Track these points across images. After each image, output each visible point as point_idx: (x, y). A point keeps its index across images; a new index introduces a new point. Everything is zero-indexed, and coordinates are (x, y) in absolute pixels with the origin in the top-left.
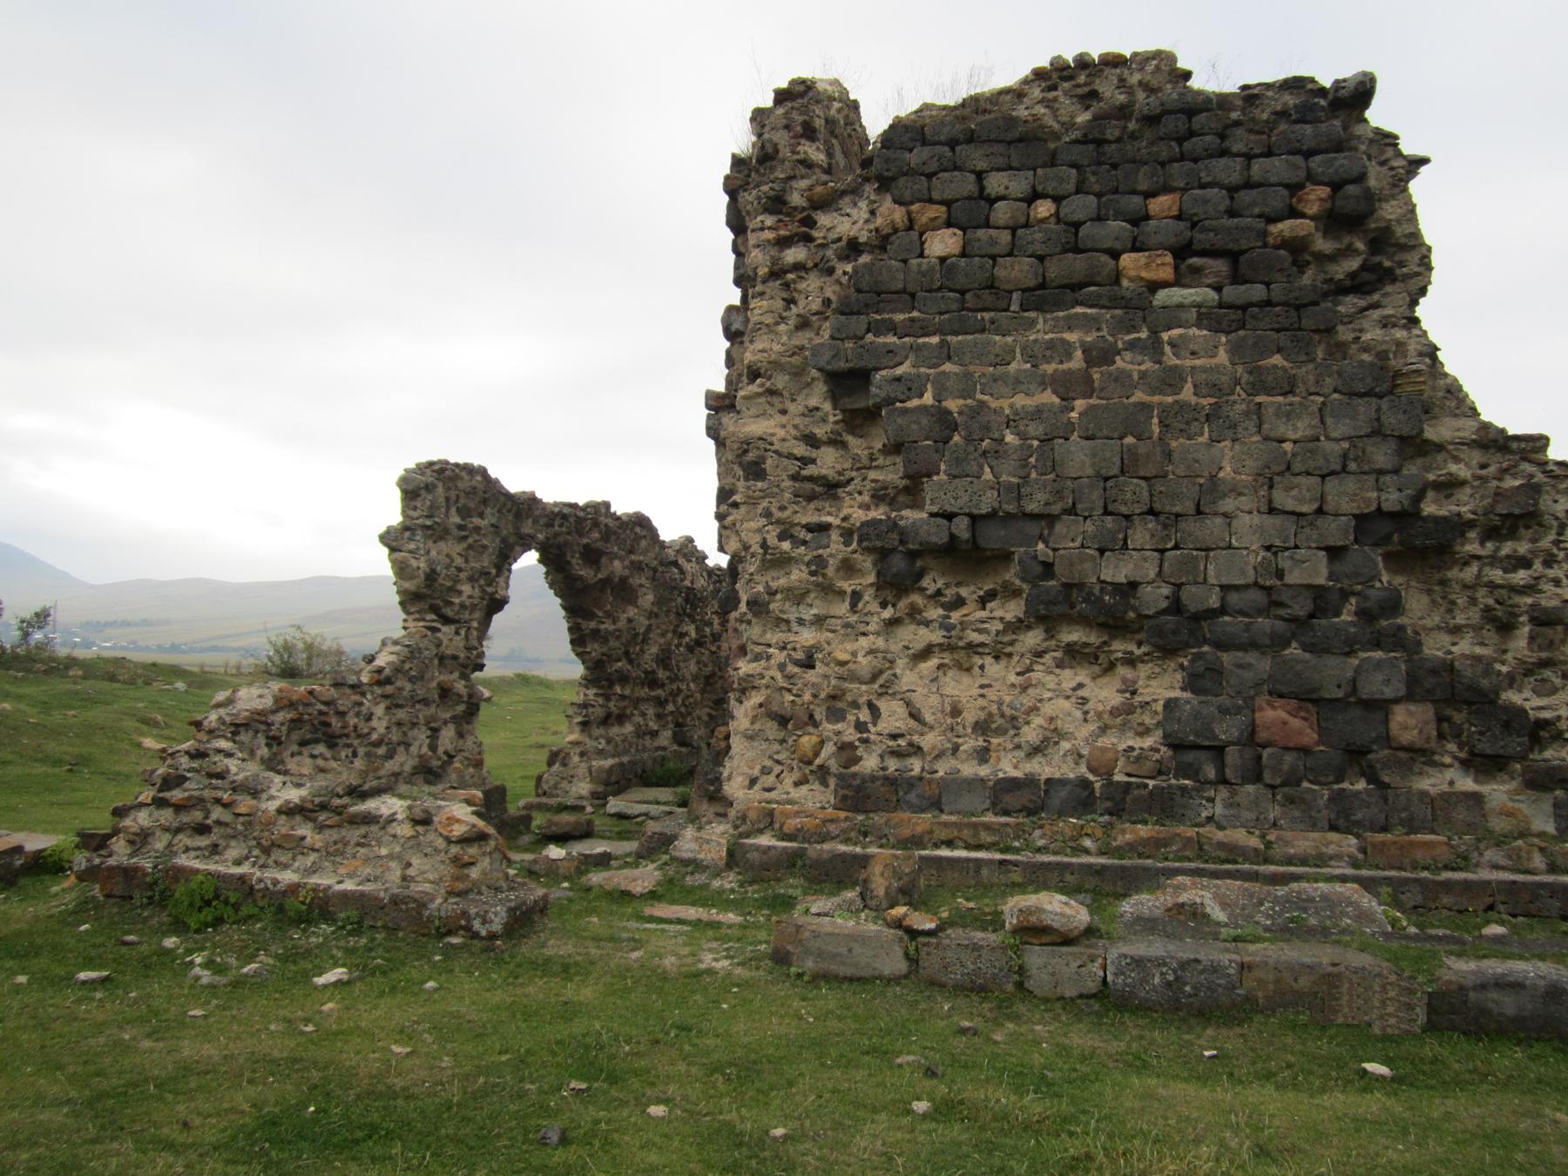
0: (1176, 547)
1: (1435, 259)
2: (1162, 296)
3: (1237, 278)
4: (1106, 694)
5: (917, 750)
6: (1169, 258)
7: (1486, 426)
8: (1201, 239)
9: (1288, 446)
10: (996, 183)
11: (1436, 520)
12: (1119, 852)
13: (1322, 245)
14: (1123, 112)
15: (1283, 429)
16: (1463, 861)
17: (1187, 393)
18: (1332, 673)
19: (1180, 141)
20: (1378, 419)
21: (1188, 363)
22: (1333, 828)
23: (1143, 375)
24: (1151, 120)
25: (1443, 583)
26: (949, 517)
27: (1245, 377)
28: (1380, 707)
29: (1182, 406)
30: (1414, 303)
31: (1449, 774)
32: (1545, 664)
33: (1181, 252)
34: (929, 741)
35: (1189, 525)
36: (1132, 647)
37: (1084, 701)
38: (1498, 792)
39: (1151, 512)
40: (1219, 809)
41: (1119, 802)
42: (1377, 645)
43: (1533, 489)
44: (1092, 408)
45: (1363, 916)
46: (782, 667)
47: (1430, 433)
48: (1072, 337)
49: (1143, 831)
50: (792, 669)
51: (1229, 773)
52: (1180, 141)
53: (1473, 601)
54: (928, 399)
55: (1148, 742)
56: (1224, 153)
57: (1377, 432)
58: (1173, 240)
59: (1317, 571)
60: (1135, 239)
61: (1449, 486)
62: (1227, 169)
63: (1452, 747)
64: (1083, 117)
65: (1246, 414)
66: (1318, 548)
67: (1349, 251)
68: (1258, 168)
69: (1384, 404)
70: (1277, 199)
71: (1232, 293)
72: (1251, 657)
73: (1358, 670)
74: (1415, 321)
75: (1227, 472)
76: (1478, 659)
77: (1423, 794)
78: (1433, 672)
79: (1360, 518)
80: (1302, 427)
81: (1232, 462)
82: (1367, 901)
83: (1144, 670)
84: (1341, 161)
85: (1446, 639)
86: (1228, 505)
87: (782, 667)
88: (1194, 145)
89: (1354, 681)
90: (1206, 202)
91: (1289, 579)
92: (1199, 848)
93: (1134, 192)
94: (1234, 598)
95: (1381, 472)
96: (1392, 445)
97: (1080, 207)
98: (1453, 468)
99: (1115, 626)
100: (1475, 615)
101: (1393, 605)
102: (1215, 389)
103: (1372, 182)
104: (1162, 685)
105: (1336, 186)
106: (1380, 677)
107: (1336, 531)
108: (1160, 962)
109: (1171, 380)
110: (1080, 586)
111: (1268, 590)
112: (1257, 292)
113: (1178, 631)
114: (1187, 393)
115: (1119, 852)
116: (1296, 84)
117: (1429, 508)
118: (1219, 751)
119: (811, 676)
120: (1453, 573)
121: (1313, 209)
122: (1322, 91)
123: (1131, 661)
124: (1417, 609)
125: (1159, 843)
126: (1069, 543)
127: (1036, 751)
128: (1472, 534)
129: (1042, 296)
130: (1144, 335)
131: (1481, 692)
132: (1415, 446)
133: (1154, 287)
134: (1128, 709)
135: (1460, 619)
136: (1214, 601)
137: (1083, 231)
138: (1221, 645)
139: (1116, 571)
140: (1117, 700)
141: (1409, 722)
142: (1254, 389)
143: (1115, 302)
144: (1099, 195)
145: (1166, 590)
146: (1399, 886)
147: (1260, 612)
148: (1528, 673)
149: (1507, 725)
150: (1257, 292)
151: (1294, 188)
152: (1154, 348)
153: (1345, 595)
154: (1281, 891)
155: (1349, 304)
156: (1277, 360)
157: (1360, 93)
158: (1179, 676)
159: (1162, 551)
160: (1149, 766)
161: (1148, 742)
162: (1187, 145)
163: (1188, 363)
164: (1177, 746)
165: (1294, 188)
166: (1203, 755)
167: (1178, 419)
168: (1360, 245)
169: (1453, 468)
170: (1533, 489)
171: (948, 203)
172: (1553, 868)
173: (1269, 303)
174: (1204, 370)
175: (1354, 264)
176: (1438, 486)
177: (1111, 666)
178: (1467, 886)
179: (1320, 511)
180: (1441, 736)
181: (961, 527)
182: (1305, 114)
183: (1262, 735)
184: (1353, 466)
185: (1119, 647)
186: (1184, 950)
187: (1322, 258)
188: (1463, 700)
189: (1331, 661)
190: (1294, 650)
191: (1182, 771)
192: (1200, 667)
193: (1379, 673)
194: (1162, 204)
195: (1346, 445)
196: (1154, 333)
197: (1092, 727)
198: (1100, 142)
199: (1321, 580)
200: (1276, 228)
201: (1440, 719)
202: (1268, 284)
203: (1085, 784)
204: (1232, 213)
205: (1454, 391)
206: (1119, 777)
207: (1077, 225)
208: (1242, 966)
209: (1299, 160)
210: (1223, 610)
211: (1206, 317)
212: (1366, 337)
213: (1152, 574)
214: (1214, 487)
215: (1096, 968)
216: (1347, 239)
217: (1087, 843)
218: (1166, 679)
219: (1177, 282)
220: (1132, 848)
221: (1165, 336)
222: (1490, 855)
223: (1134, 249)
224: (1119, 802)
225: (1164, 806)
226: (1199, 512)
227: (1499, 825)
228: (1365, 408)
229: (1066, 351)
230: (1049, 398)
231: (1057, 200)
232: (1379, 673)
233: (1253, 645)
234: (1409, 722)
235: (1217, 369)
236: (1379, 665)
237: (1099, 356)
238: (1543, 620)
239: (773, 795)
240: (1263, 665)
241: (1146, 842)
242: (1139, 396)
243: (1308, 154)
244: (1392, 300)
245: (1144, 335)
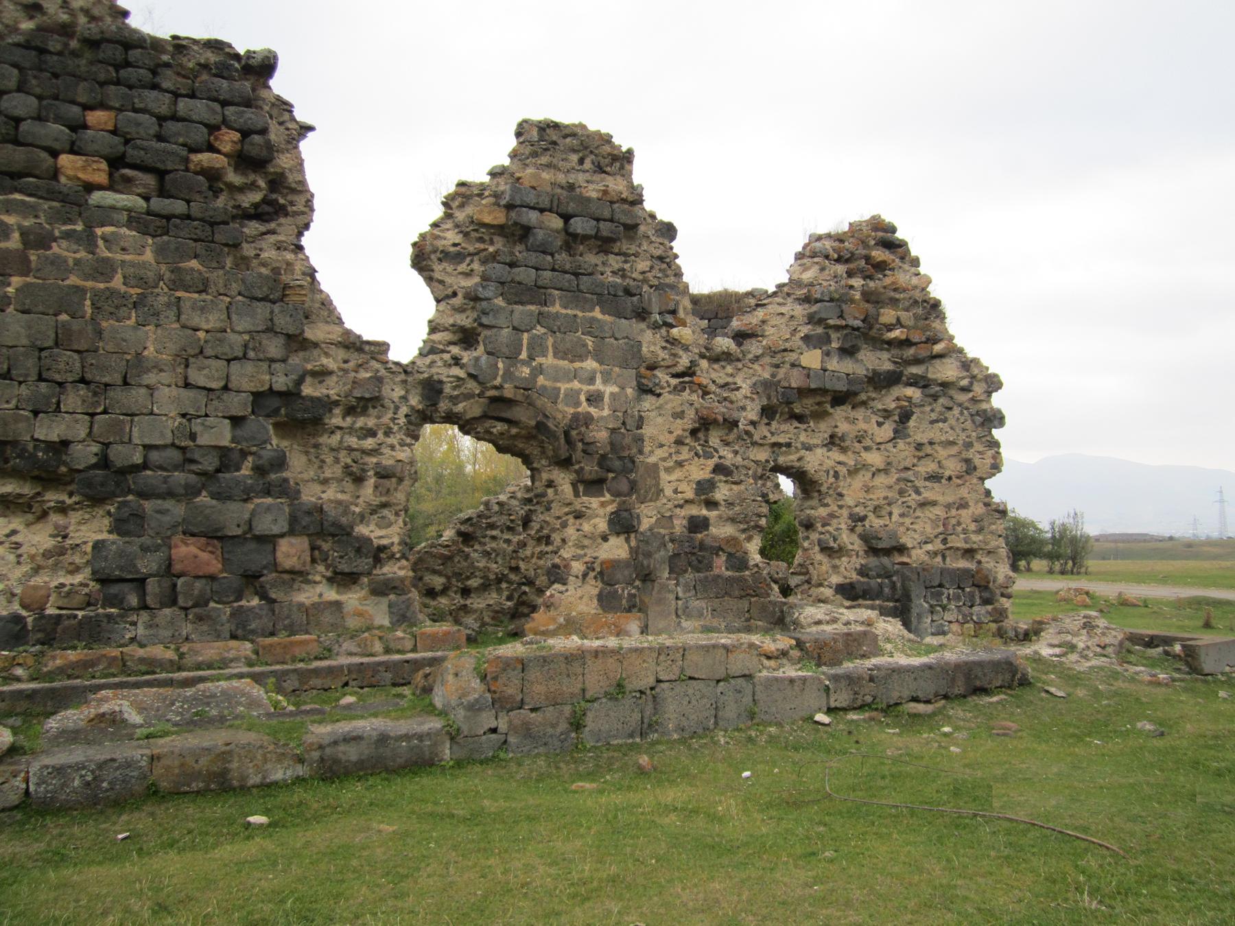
0: (105, 412)
1: (316, 203)
2: (97, 197)
3: (163, 193)
4: (39, 538)
6: (104, 165)
7: (348, 333)
8: (132, 154)
9: (201, 334)
11: (312, 399)
12: (50, 676)
13: (233, 177)
14: (66, 30)
15: (197, 320)
16: (328, 653)
17: (117, 282)
18: (233, 515)
19: (117, 67)
20: (271, 320)
21: (119, 257)
22: (234, 637)
23: (77, 262)
24: (93, 44)
25: (316, 446)
27: (167, 275)
28: (269, 541)
29: (112, 293)
30: (300, 234)
31: (319, 589)
32: (384, 505)
33: (116, 162)
35: (117, 394)
36: (64, 497)
37: (18, 545)
38: (353, 599)
39: (83, 380)
40: (141, 630)
41: (51, 633)
42: (268, 493)
43: (379, 380)
44: (27, 285)
45: (253, 703)
47: (309, 334)
48: (11, 220)
49: (72, 655)
51: (150, 600)
52: (117, 67)
53: (337, 460)
55: (78, 579)
56: (155, 87)
57: (270, 330)
58: (107, 151)
59: (220, 434)
60: (73, 143)
61: (322, 374)
62: (159, 102)
63: (321, 568)
64: (27, 25)
65: (168, 305)
66: (224, 417)
67: (253, 186)
68: (183, 105)
69: (277, 308)
70: (199, 135)
71: (157, 204)
72: (168, 504)
73: (253, 513)
74: (300, 248)
75: (150, 352)
76: (339, 503)
77: (301, 605)
78: (309, 513)
79: (257, 395)
80: (213, 320)
81: (155, 343)
82: (257, 691)
83: (75, 517)
84: (249, 114)
85: (317, 488)
86: (151, 378)
89: (250, 522)
90: (138, 124)
91: (200, 441)
92: (123, 665)
93: (73, 102)
94: (154, 456)
95: (272, 360)
96: (280, 341)
98: (325, 361)
99: (47, 478)
100: (338, 471)
101: (280, 462)
102: (142, 281)
103: (272, 137)
104: (90, 529)
105: (245, 134)
106: (269, 517)
107: (238, 404)
108: (79, 767)
109: (103, 270)
110: (14, 443)
111: (183, 449)
112: (179, 207)
113: (106, 482)
114: (117, 282)
115: (50, 676)
116: (215, 45)
117: (308, 390)
118: (141, 582)
120: (324, 439)
121: (227, 148)
122: (237, 57)
123: (63, 509)
124: (298, 466)
125: (86, 665)
128: (337, 411)
130: (79, 227)
131: (340, 527)
132: (297, 342)
133: (90, 188)
134: (61, 551)
135: (328, 474)
136: (138, 458)
137: (24, 126)
138: (143, 495)
139: (48, 430)
140: (49, 543)
141: (291, 551)
142: (176, 285)
143: (51, 195)
144: (40, 98)
145: (95, 448)
146: (281, 676)
147: (176, 468)
148: (373, 512)
149: (358, 551)
150: (179, 207)
151: (213, 128)
152: (88, 240)
153: (244, 454)
154: (189, 692)
155: (253, 228)
156: (194, 264)
157: (263, 67)
158: (107, 521)
159: (92, 415)
160: (78, 600)
161: (78, 579)
162: (123, 73)
163: (119, 257)
164: (104, 581)
165: (213, 128)
166: (126, 587)
167: (109, 303)
168: (262, 183)
169: (325, 361)
170: (379, 380)
172: (388, 651)
173: (188, 217)
174: (133, 264)
175: (257, 197)
176: (314, 374)
177: (44, 515)
178: (331, 671)
179: (226, 388)
180: (313, 561)
182: (222, 71)
183: (177, 568)
184: (251, 354)
185: (52, 497)
186: (99, 754)
187: (231, 188)
188: (327, 532)
189: (233, 506)
190: (204, 499)
191: (109, 601)
192: (126, 512)
193: (269, 515)
194: (97, 118)
195: (247, 337)
196: (89, 227)
197: (25, 568)
198: (42, 51)
199: (225, 442)
201: (313, 548)
202: (188, 202)
203: (17, 619)
204: (160, 138)
205: (326, 304)
206: (51, 611)
207: (18, 120)
208: (152, 758)
209: (217, 106)
210: (145, 466)
211: (135, 220)
212: (264, 255)
213: (83, 434)
214: (138, 363)
215: (18, 783)
216: (252, 177)
217: (19, 672)
218: (95, 524)
219: (110, 187)
220: (61, 671)
221: (99, 231)
222: (348, 645)
223: (72, 151)
224: (51, 633)
225: (92, 632)
226: (125, 383)
227: (352, 623)
228: (262, 310)
232: (269, 515)
233: (170, 494)
234: (291, 551)
235: (143, 265)
236: (269, 509)
237: (37, 240)
238: (383, 474)
240: (178, 510)
241: (73, 665)
242: (73, 280)
243: (225, 104)
244: (285, 227)
245: (79, 227)
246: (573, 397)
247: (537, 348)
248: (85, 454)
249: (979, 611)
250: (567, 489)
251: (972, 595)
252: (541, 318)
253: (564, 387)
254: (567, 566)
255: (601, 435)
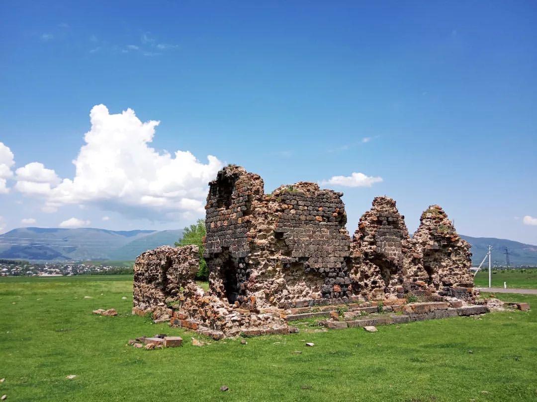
3: (329, 221)
5: (289, 298)
10: (300, 203)
26: (295, 257)
33: (323, 216)
34: (291, 296)
46: (267, 285)
50: (269, 285)
54: (292, 238)
56: (327, 202)
87: (267, 285)
88: (324, 200)
97: (311, 208)
119: (273, 286)
123: (316, 280)
126: (310, 262)
127: (305, 296)
129: (307, 222)
136: (329, 270)
167: (324, 242)
171: (293, 205)
181: (297, 259)
194: (320, 209)
200: (334, 214)
229: (309, 231)
230: (308, 238)
231: (308, 207)
239: (265, 309)
246: (391, 254)
247: (385, 245)
248: (322, 270)
249: (469, 298)
250: (389, 273)
251: (468, 295)
252: (385, 239)
253: (390, 252)
254: (390, 289)
255: (396, 262)
